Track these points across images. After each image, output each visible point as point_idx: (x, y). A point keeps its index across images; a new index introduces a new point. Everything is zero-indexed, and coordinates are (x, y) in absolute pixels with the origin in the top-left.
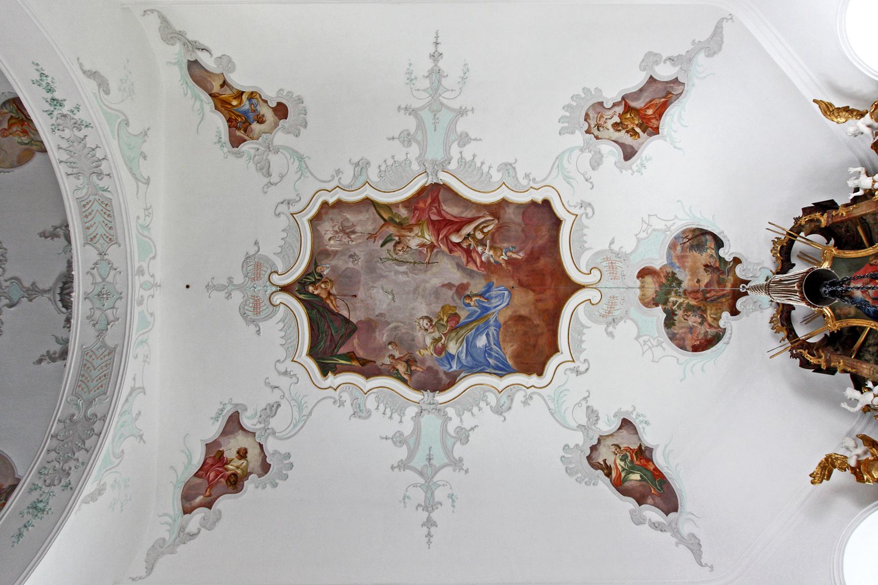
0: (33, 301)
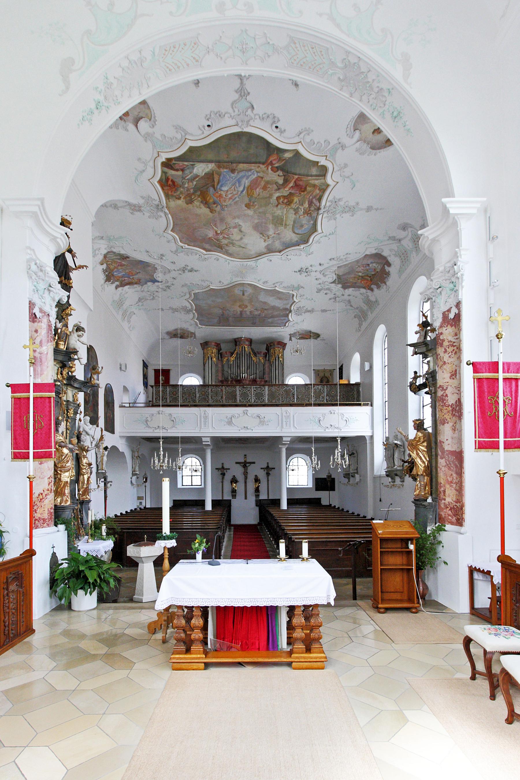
0: (249, 91)
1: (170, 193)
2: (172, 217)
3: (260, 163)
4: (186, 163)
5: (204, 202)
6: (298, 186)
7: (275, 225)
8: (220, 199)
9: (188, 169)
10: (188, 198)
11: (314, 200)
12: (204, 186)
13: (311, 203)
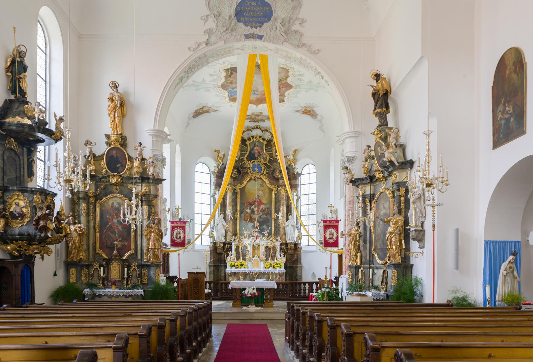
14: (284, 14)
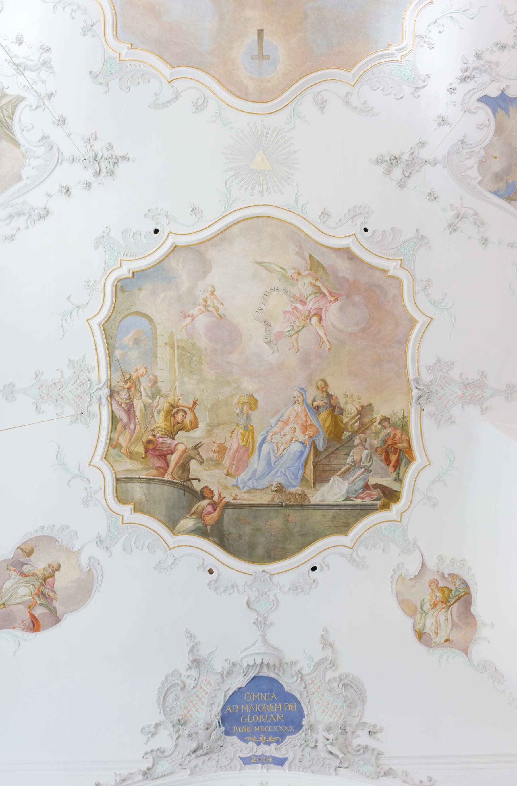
0: (254, 625)
1: (398, 432)
2: (405, 367)
3: (234, 506)
4: (359, 501)
5: (337, 412)
6: (161, 455)
7: (193, 345)
8: (307, 422)
9: (356, 491)
10: (366, 420)
11: (125, 420)
12: (333, 453)
13: (130, 410)
14: (331, 716)
